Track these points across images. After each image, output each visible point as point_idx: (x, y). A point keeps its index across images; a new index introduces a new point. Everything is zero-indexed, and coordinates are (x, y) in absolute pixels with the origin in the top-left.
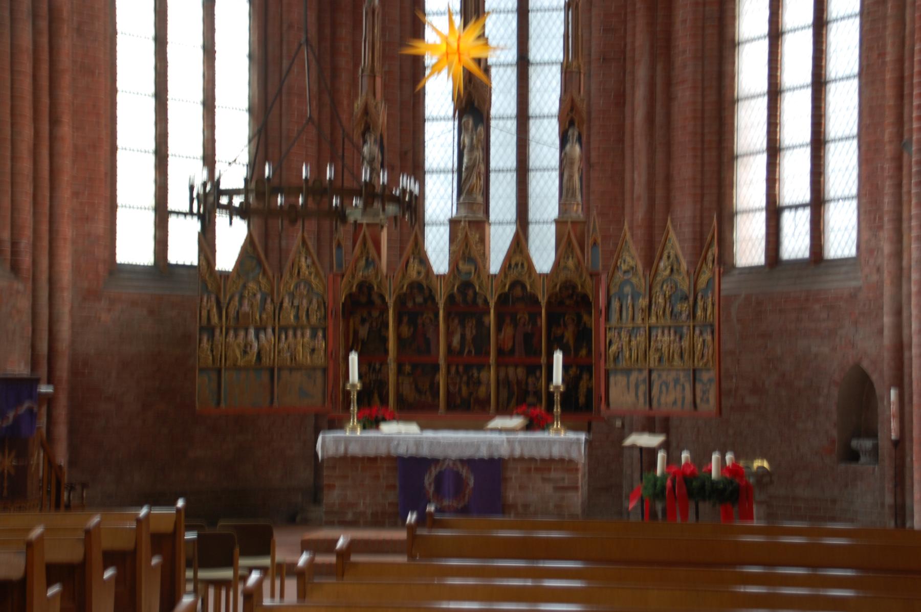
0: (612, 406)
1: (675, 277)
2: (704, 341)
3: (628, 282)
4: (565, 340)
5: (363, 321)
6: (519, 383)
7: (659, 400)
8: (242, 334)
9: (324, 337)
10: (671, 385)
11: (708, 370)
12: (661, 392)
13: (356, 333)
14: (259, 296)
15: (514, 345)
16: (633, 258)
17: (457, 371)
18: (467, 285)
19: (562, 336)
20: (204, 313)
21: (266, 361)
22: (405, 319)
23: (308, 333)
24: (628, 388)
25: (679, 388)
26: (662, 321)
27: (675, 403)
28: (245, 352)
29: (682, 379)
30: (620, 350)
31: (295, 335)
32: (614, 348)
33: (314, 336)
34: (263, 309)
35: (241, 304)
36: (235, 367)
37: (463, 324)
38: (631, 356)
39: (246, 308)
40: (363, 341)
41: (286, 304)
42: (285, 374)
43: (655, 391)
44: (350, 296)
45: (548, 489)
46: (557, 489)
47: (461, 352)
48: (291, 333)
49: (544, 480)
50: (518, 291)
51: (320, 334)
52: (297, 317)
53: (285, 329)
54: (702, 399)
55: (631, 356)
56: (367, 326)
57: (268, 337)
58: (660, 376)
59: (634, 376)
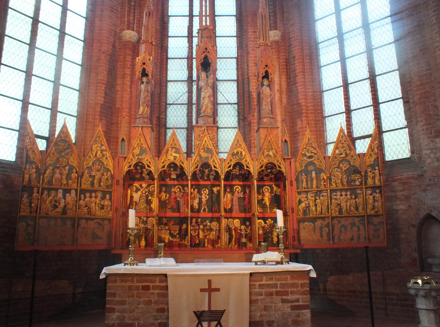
0: (302, 242)
1: (349, 158)
2: (374, 197)
3: (312, 163)
4: (264, 203)
5: (137, 190)
6: (235, 229)
7: (339, 237)
8: (53, 193)
9: (110, 199)
10: (349, 227)
11: (378, 216)
12: (341, 232)
13: (132, 197)
14: (67, 168)
15: (232, 205)
16: (315, 149)
17: (197, 222)
18: (206, 165)
19: (263, 200)
20: (27, 176)
21: (70, 214)
22: (164, 189)
23: (100, 195)
24: (314, 231)
25: (355, 229)
26: (340, 187)
27: (352, 239)
28: (55, 207)
29: (357, 223)
30: (308, 207)
31: (91, 197)
32: (303, 205)
33: (103, 198)
34: (69, 177)
35: (54, 173)
36: (47, 217)
37: (199, 192)
38: (316, 210)
39: (57, 175)
40: (136, 202)
41: (86, 175)
42: (83, 222)
43: (336, 232)
44: (129, 172)
45: (287, 308)
46: (294, 308)
47: (198, 211)
48: (88, 195)
49: (283, 301)
50: (236, 171)
51: (108, 196)
52: (92, 184)
53: (83, 192)
54: (374, 235)
55: (316, 210)
56: (139, 193)
57: (71, 197)
58: (339, 222)
59: (319, 223)
